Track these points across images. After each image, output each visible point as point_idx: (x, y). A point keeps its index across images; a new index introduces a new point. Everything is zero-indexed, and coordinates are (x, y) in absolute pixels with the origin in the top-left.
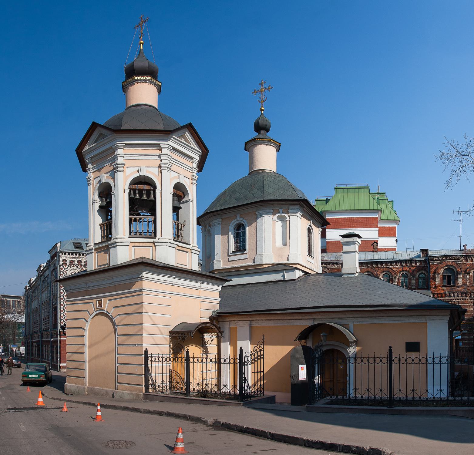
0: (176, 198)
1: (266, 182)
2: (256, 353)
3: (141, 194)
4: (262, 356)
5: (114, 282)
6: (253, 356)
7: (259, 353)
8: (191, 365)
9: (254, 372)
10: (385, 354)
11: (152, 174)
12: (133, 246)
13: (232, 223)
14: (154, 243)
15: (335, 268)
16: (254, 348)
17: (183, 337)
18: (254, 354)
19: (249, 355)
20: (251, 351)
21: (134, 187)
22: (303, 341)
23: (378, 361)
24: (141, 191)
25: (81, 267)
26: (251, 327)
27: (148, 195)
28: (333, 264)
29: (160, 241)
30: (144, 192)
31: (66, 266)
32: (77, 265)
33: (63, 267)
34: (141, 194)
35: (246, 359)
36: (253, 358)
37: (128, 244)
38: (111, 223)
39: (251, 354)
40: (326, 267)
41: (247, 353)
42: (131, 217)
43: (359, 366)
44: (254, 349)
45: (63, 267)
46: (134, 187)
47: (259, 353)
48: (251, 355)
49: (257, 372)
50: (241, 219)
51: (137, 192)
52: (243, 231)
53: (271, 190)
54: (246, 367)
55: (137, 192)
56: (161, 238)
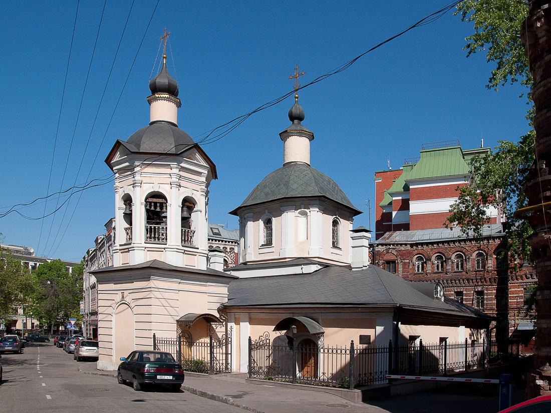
0: (185, 209)
1: (292, 177)
3: (155, 207)
10: (349, 347)
11: (165, 190)
14: (164, 249)
15: (403, 249)
21: (150, 200)
23: (339, 351)
24: (155, 203)
27: (161, 208)
28: (401, 245)
29: (170, 247)
30: (158, 205)
34: (155, 207)
37: (144, 249)
40: (394, 249)
43: (330, 355)
46: (150, 200)
53: (295, 186)
55: (153, 204)
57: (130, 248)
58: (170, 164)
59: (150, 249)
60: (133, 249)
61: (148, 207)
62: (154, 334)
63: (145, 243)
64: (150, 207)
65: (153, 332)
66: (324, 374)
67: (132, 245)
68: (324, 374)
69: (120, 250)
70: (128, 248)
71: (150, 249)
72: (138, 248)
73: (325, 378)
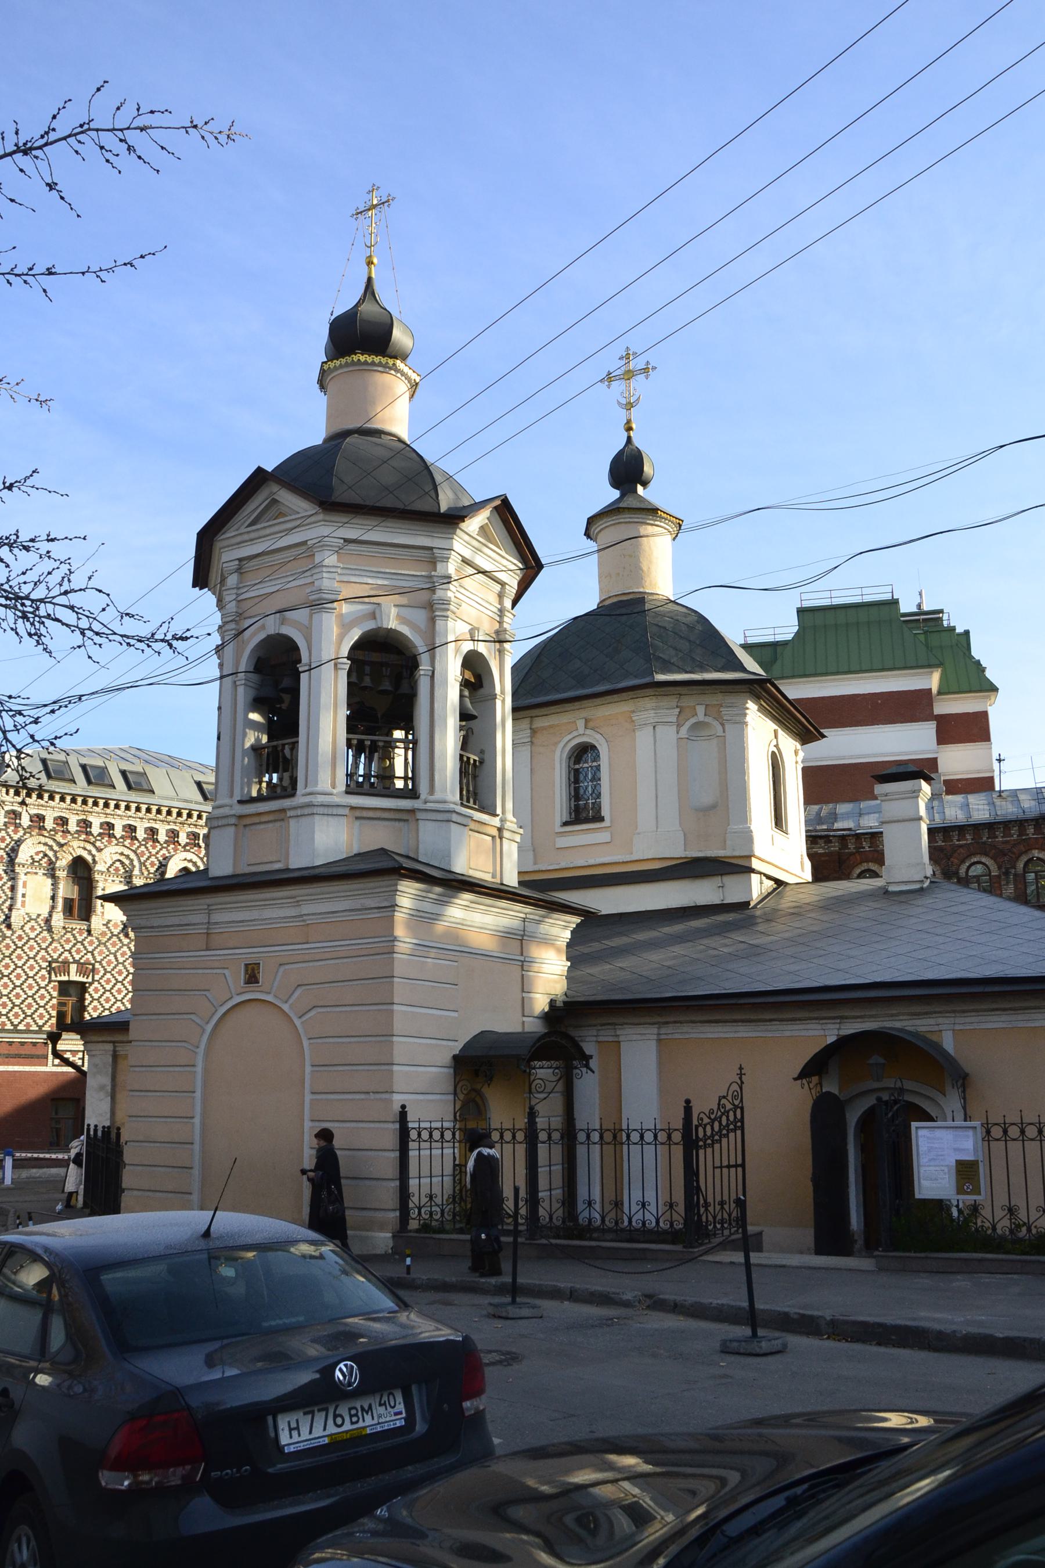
2: (723, 1114)
4: (739, 1124)
5: (302, 916)
6: (716, 1125)
7: (731, 1114)
8: (581, 1151)
9: (721, 1167)
12: (357, 818)
13: (562, 744)
14: (412, 811)
16: (720, 1101)
17: (482, 1066)
18: (720, 1118)
19: (706, 1120)
20: (712, 1111)
22: (815, 1079)
25: (64, 838)
26: (659, 1041)
31: (15, 832)
32: (54, 830)
33: (7, 833)
35: (701, 1129)
36: (716, 1128)
38: (280, 748)
39: (713, 1117)
41: (702, 1115)
42: (351, 736)
44: (719, 1104)
45: (7, 833)
47: (731, 1114)
48: (713, 1121)
49: (729, 1167)
50: (588, 732)
51: (367, 669)
52: (595, 764)
54: (701, 1152)
55: (367, 669)
56: (431, 798)
57: (295, 808)
58: (431, 549)
59: (365, 814)
60: (306, 811)
61: (354, 679)
62: (403, 1107)
63: (347, 792)
64: (360, 677)
65: (398, 1099)
66: (643, 1205)
67: (299, 799)
68: (643, 1205)
69: (241, 817)
70: (283, 811)
71: (365, 814)
72: (326, 811)
73: (648, 1216)
